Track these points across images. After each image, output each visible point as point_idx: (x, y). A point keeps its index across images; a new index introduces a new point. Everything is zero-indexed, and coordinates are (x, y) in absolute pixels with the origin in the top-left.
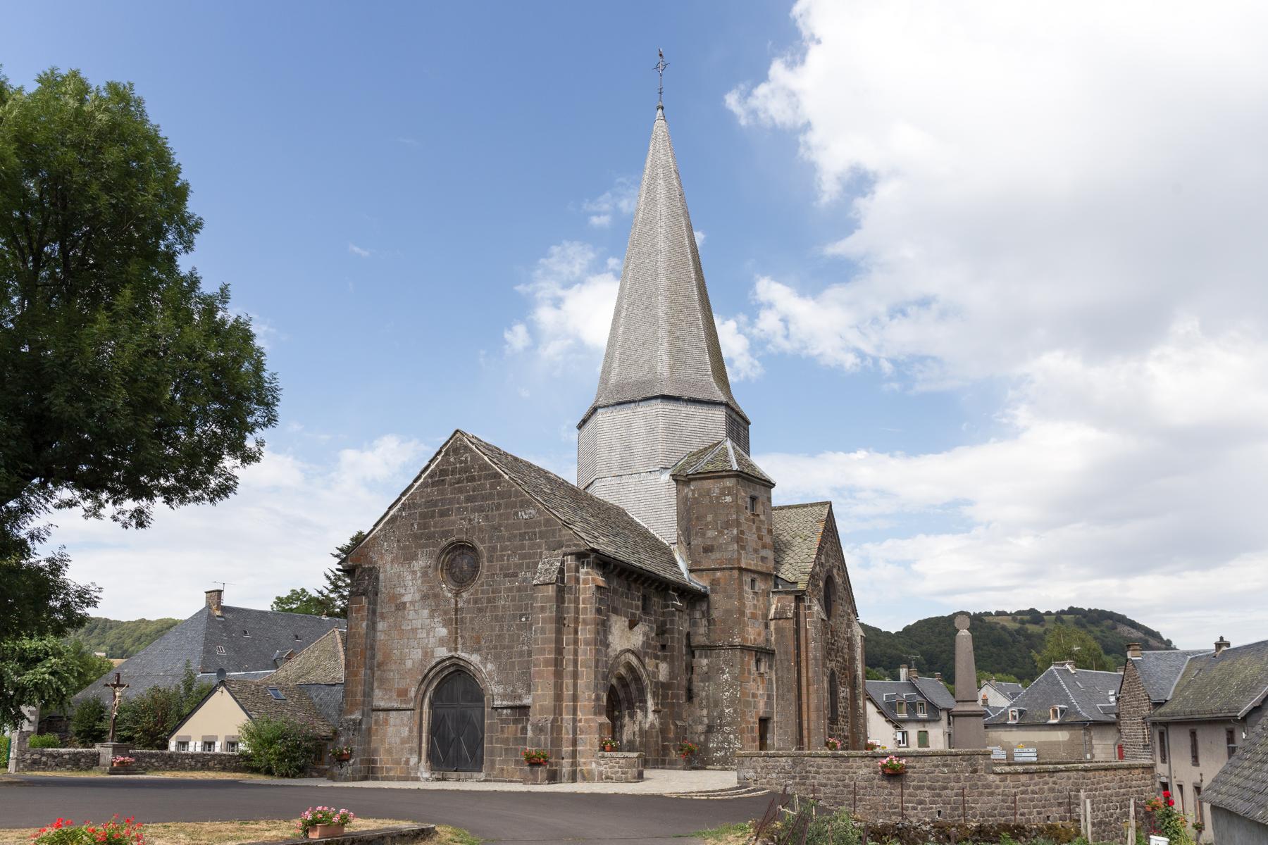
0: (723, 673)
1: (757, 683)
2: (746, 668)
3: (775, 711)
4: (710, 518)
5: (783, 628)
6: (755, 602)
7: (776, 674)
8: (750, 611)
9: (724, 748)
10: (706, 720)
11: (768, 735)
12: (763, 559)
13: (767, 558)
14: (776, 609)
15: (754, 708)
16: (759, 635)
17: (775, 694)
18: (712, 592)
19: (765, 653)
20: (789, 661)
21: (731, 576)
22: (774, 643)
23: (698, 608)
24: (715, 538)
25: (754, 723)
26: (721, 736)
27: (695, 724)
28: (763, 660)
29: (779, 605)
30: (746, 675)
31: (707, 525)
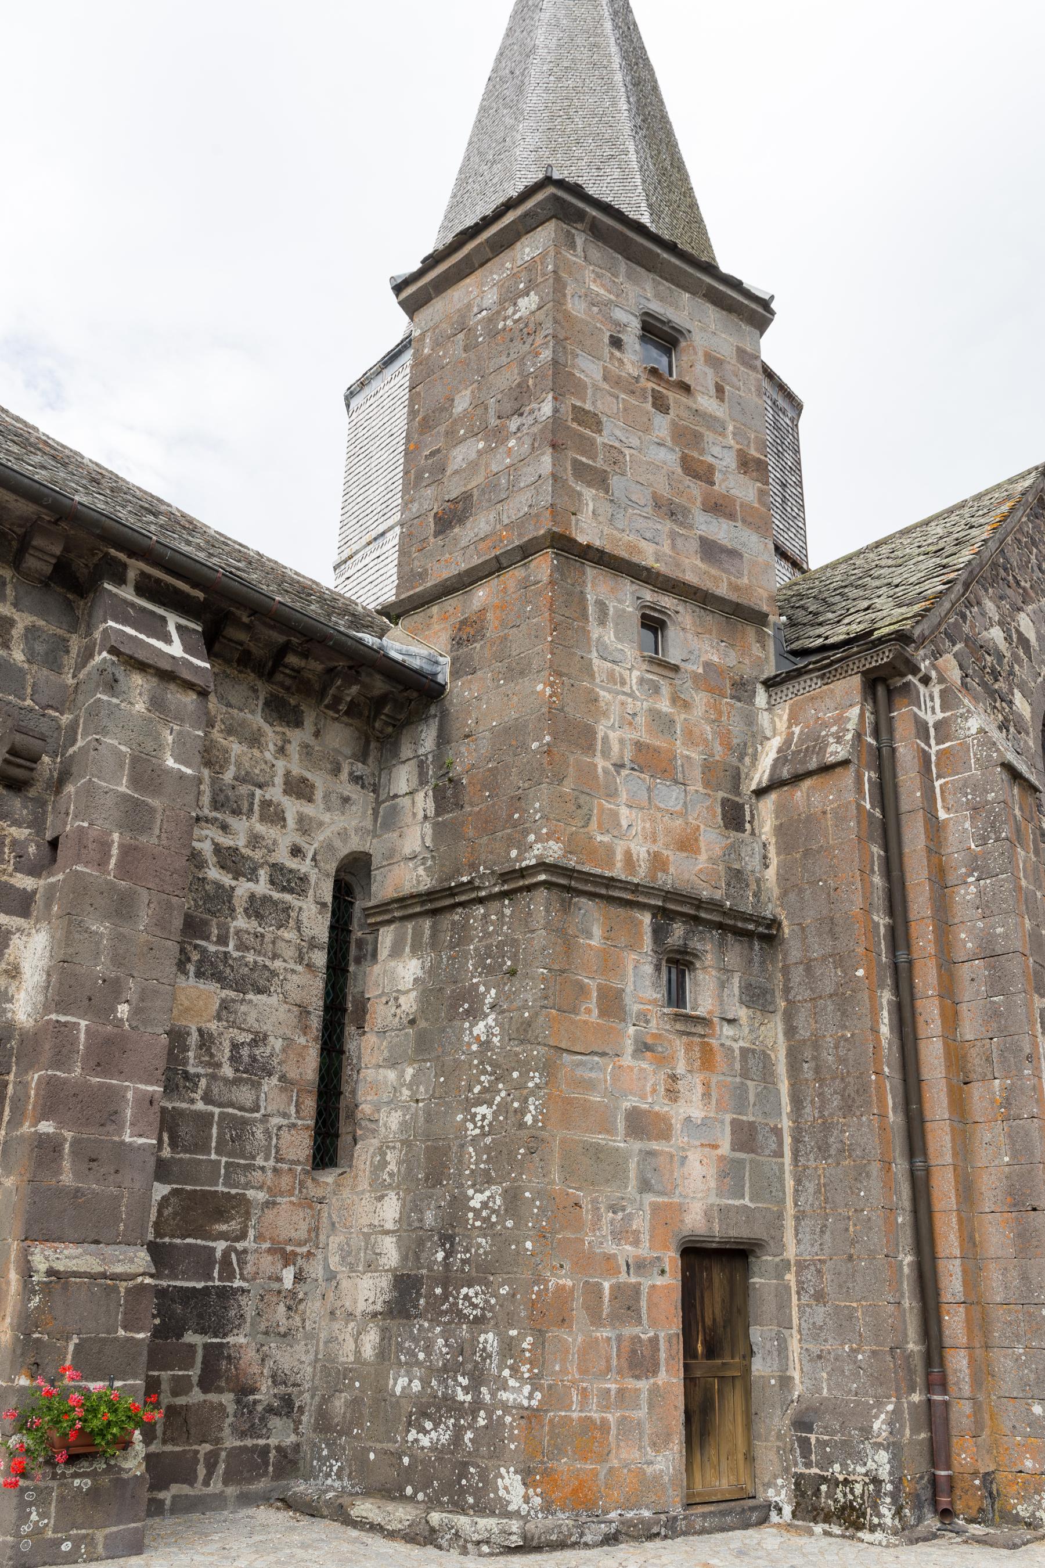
0: (474, 1014)
1: (663, 1061)
2: (592, 984)
3: (790, 1210)
4: (462, 404)
5: (810, 819)
6: (664, 706)
7: (790, 1031)
8: (630, 735)
9: (450, 1405)
10: (390, 1252)
11: (756, 1334)
12: (710, 550)
13: (734, 554)
14: (788, 742)
15: (645, 1186)
16: (687, 844)
17: (786, 1124)
18: (455, 674)
19: (720, 926)
20: (840, 960)
21: (525, 584)
22: (776, 892)
23: (406, 752)
24: (473, 466)
25: (640, 1266)
26: (446, 1335)
27: (352, 1270)
28: (709, 959)
29: (797, 730)
30: (590, 1012)
31: (450, 433)
